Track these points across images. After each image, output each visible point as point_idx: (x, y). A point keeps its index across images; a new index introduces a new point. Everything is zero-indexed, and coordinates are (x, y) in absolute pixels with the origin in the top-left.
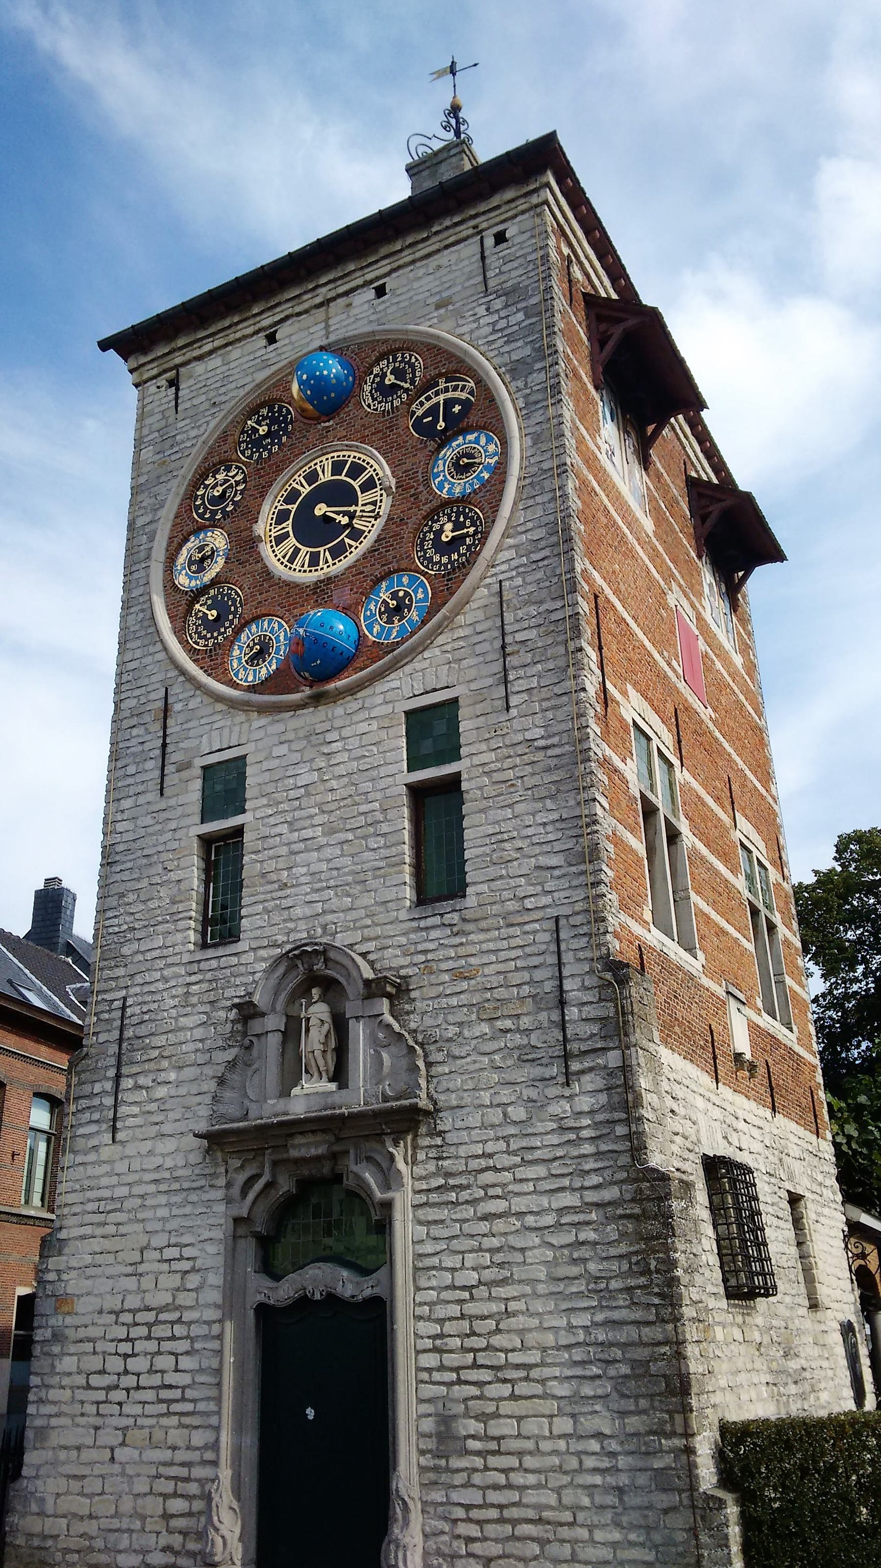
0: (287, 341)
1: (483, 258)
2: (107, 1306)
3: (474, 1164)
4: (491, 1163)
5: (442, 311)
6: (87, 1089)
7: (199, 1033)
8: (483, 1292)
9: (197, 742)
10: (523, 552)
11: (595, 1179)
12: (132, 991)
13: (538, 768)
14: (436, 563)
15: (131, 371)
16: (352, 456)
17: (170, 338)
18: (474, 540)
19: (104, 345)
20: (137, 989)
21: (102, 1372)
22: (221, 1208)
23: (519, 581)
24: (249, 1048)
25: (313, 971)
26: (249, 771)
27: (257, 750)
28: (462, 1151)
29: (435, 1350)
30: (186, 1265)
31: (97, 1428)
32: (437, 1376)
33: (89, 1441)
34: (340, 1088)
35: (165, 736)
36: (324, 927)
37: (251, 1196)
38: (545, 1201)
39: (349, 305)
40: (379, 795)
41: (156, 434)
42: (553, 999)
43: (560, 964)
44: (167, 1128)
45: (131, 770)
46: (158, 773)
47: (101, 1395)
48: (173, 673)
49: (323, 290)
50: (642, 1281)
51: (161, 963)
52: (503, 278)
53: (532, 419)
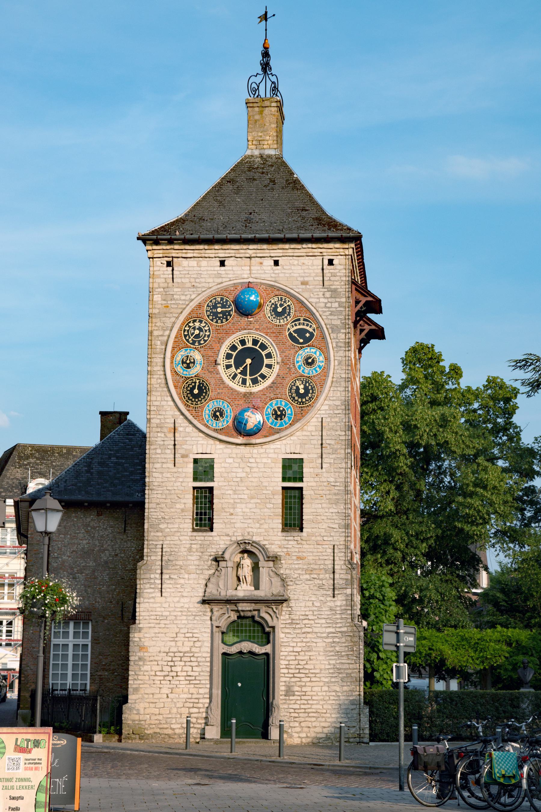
0: (230, 268)
1: (323, 269)
2: (162, 650)
3: (302, 617)
5: (304, 287)
6: (147, 576)
7: (197, 563)
8: (302, 653)
9: (191, 447)
12: (166, 542)
16: (262, 340)
20: (168, 542)
21: (162, 671)
23: (329, 420)
27: (219, 458)
28: (298, 613)
29: (287, 668)
30: (196, 639)
32: (286, 675)
34: (255, 589)
35: (175, 440)
36: (249, 533)
38: (324, 630)
40: (271, 489)
41: (162, 290)
44: (185, 594)
45: (159, 451)
46: (173, 456)
47: (162, 678)
48: (179, 413)
50: (351, 653)
51: (179, 534)
52: (331, 283)
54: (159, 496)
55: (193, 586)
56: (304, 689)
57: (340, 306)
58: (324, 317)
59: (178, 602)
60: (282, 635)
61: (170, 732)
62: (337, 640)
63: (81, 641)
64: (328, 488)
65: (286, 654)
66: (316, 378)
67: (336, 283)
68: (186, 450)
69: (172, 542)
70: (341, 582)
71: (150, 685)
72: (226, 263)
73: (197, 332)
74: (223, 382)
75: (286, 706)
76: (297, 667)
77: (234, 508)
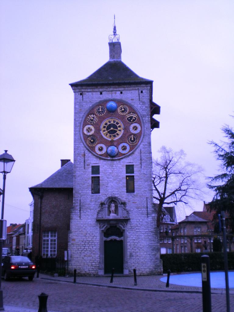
1: (139, 94)
2: (81, 240)
3: (135, 226)
5: (132, 101)
7: (94, 206)
11: (150, 228)
12: (81, 198)
13: (145, 177)
16: (117, 121)
19: (70, 84)
21: (81, 248)
22: (99, 229)
25: (113, 200)
26: (100, 168)
29: (130, 246)
30: (93, 236)
31: (80, 255)
33: (79, 257)
35: (84, 159)
36: (113, 194)
41: (78, 103)
42: (146, 207)
43: (147, 203)
44: (89, 218)
46: (84, 165)
48: (85, 149)
51: (86, 195)
52: (142, 99)
54: (79, 180)
55: (92, 215)
56: (137, 254)
58: (140, 112)
59: (87, 221)
60: (128, 233)
61: (84, 272)
62: (150, 234)
63: (53, 238)
65: (129, 240)
67: (144, 99)
69: (84, 198)
70: (150, 211)
71: (76, 254)
72: (102, 93)
73: (92, 119)
74: (102, 137)
75: (130, 261)
76: (134, 245)
77: (108, 184)
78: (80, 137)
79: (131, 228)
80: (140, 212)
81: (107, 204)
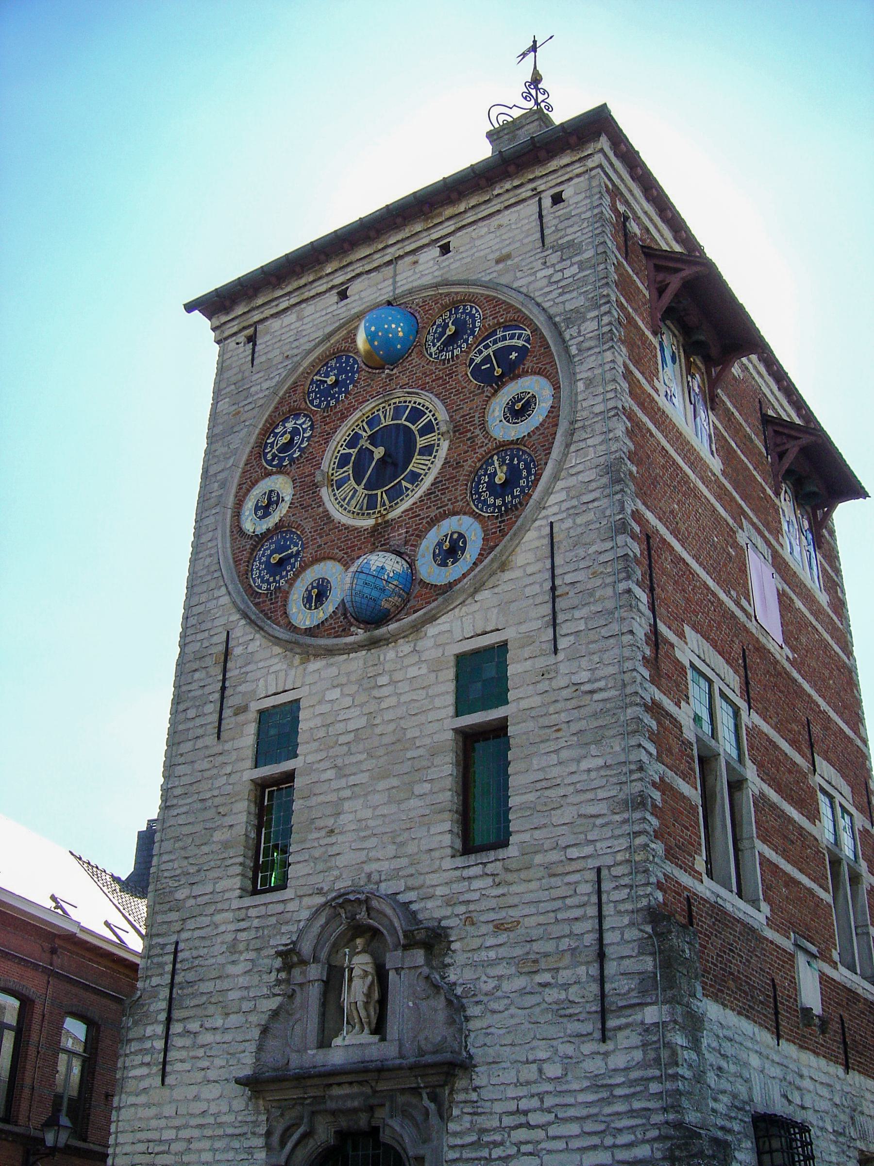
0: (357, 297)
1: (541, 217)
3: (507, 1121)
4: (523, 1119)
5: (501, 266)
7: (242, 981)
10: (573, 493)
12: (185, 935)
13: (584, 712)
14: (489, 506)
15: (214, 329)
17: (251, 297)
18: (528, 482)
19: (190, 307)
24: (291, 996)
25: (356, 919)
26: (302, 715)
28: (498, 1107)
35: (224, 680)
36: (369, 876)
37: (289, 1146)
39: (416, 262)
40: (427, 741)
41: (233, 387)
43: (600, 917)
44: (212, 1074)
45: (191, 713)
46: (216, 717)
49: (391, 250)
53: (585, 365)
57: (581, 270)
59: (197, 1098)
64: (574, 703)
66: (534, 437)
68: (244, 694)
69: (197, 933)
78: (216, 561)
79: (476, 1145)
80: (553, 995)
81: (316, 960)
